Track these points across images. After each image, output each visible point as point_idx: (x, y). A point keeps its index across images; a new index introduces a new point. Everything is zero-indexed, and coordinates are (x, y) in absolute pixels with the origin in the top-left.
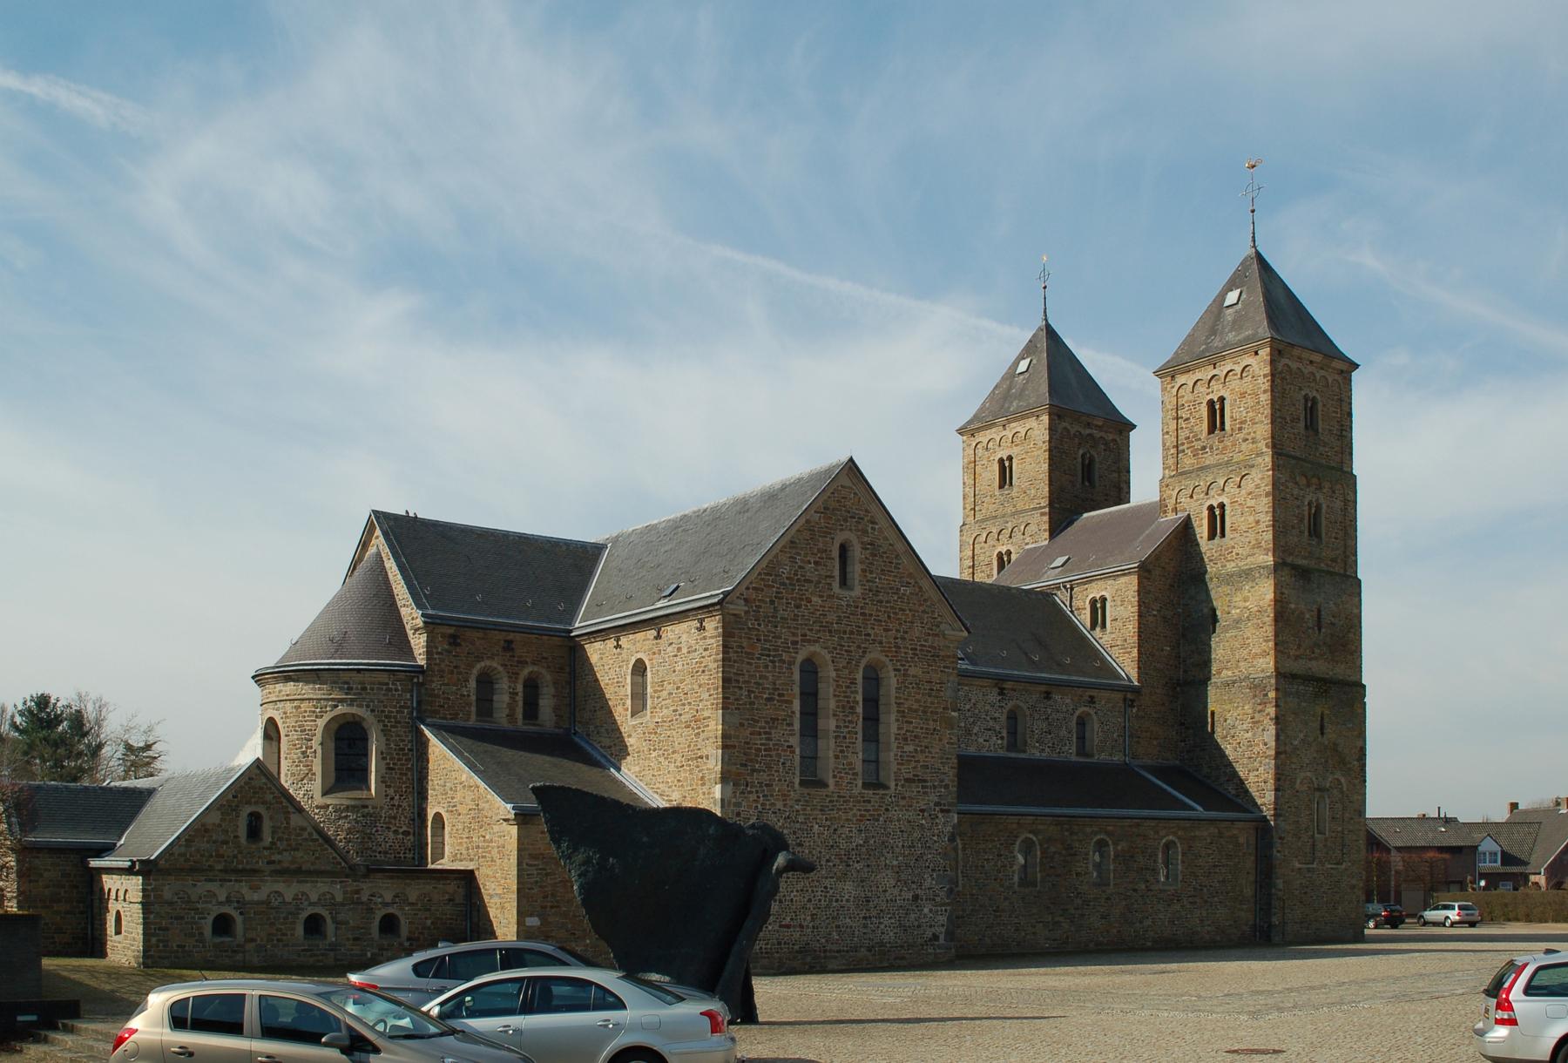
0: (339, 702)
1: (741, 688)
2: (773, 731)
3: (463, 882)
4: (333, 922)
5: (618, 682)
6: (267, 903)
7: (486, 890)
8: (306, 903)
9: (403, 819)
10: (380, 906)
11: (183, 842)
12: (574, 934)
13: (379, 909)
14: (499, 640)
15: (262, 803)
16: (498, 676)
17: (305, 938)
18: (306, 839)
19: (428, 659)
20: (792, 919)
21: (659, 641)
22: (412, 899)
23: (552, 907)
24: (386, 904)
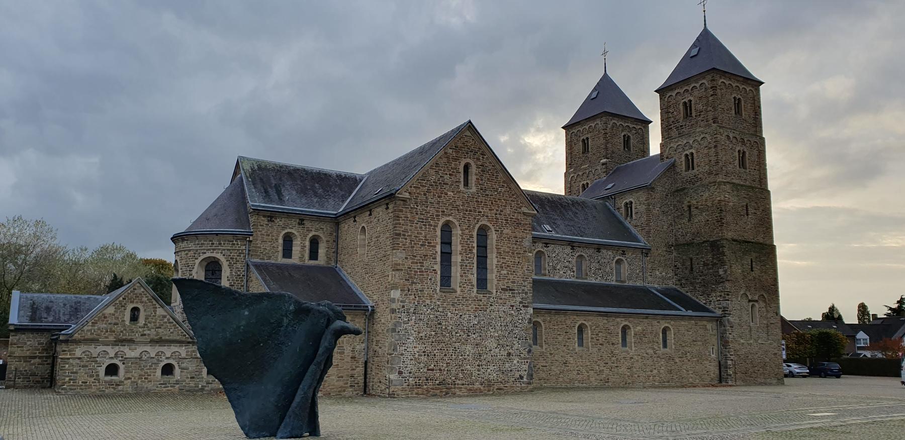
4: (179, 368)
15: (141, 302)
18: (166, 322)
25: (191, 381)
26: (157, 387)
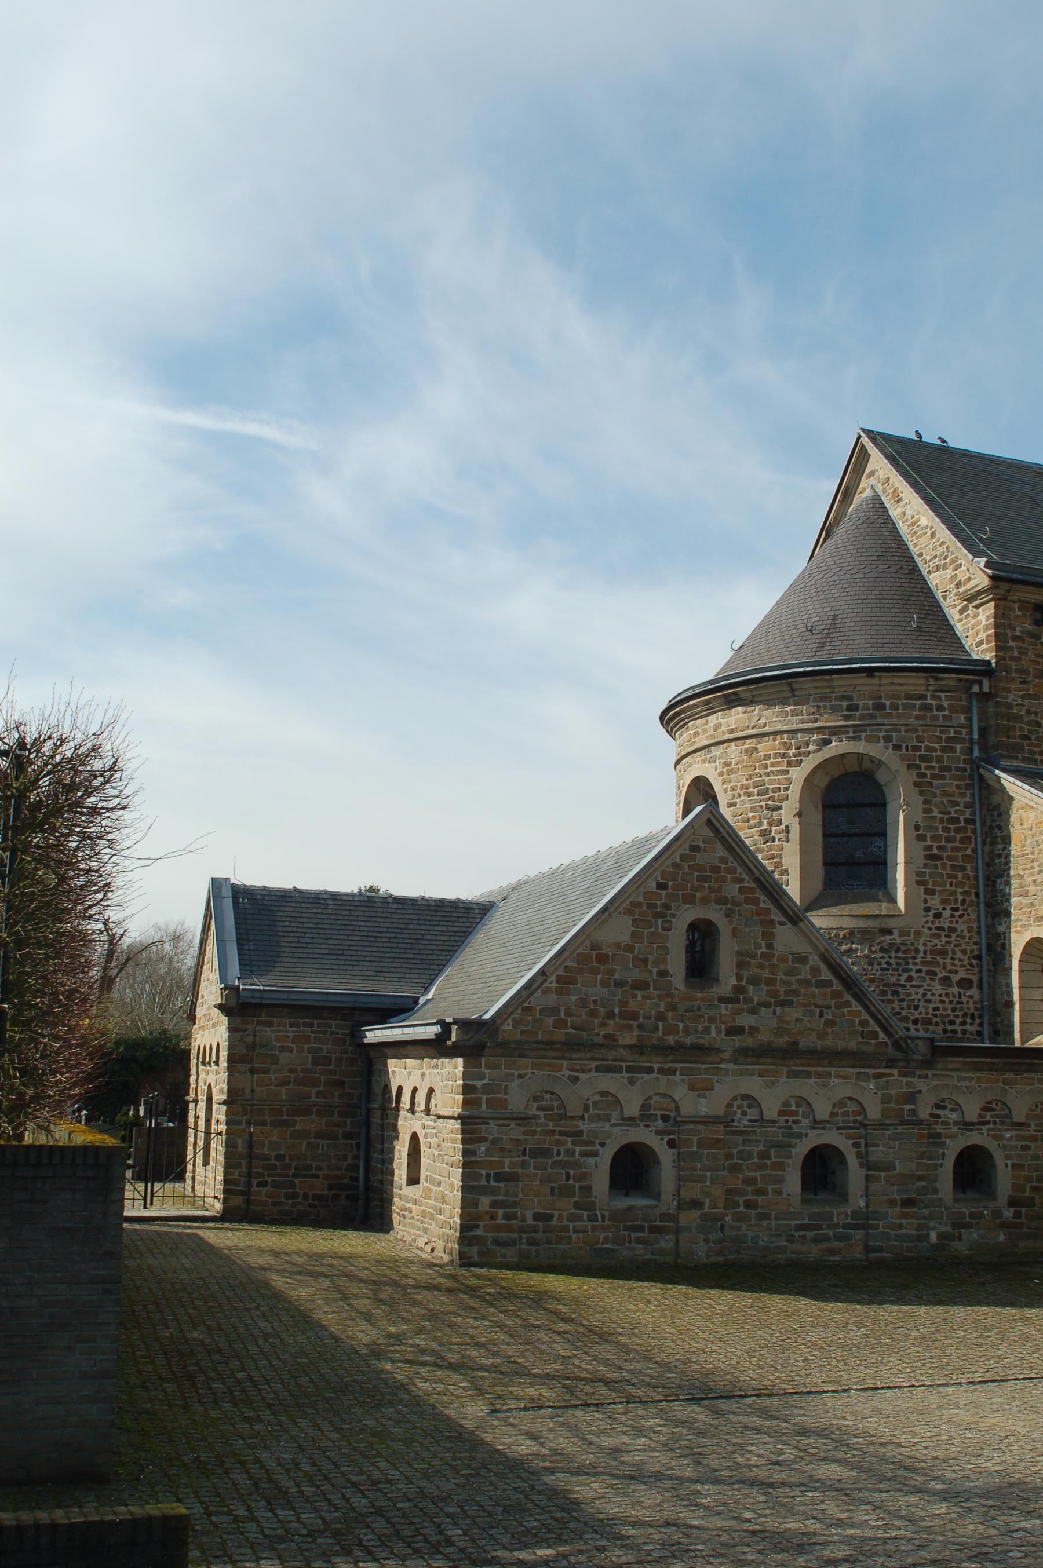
0: (832, 734)
4: (861, 1165)
6: (725, 1121)
8: (806, 1122)
9: (959, 955)
10: (955, 1129)
11: (552, 983)
13: (953, 1136)
15: (717, 903)
17: (804, 1201)
18: (806, 983)
19: (998, 648)
22: (1019, 1117)
24: (967, 1126)
25: (904, 1216)
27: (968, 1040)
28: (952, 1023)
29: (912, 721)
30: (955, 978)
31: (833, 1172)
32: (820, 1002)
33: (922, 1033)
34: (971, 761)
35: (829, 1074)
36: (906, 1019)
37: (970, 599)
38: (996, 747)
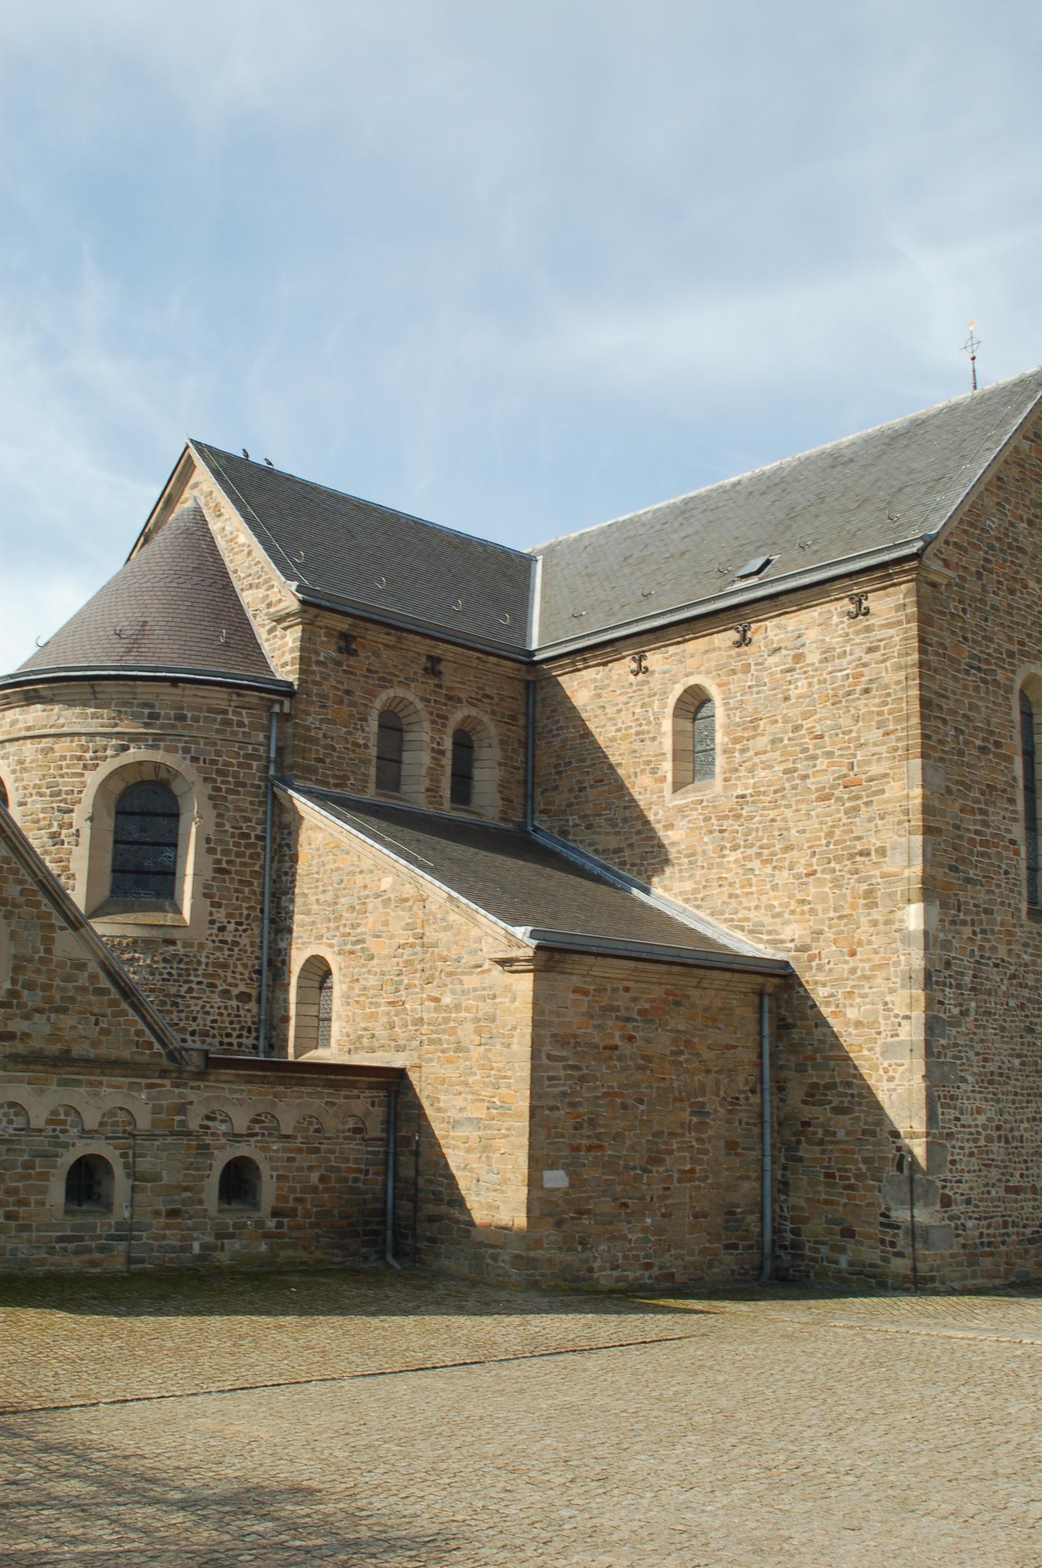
1: (945, 721)
2: (991, 810)
3: (382, 1094)
4: (128, 1175)
5: (638, 733)
7: (439, 1110)
8: (74, 1131)
9: (240, 969)
10: (223, 1141)
12: (625, 1205)
13: (221, 1148)
14: (419, 654)
16: (413, 719)
18: (83, 990)
19: (302, 671)
20: (1022, 1176)
21: (744, 649)
23: (590, 1148)
24: (235, 1137)
25: (167, 1226)
26: (51, 1251)
27: (244, 1053)
28: (229, 1035)
29: (212, 735)
30: (235, 991)
31: (99, 1183)
32: (96, 1010)
33: (198, 1045)
34: (266, 779)
35: (101, 1083)
36: (183, 1030)
37: (279, 620)
38: (292, 767)
